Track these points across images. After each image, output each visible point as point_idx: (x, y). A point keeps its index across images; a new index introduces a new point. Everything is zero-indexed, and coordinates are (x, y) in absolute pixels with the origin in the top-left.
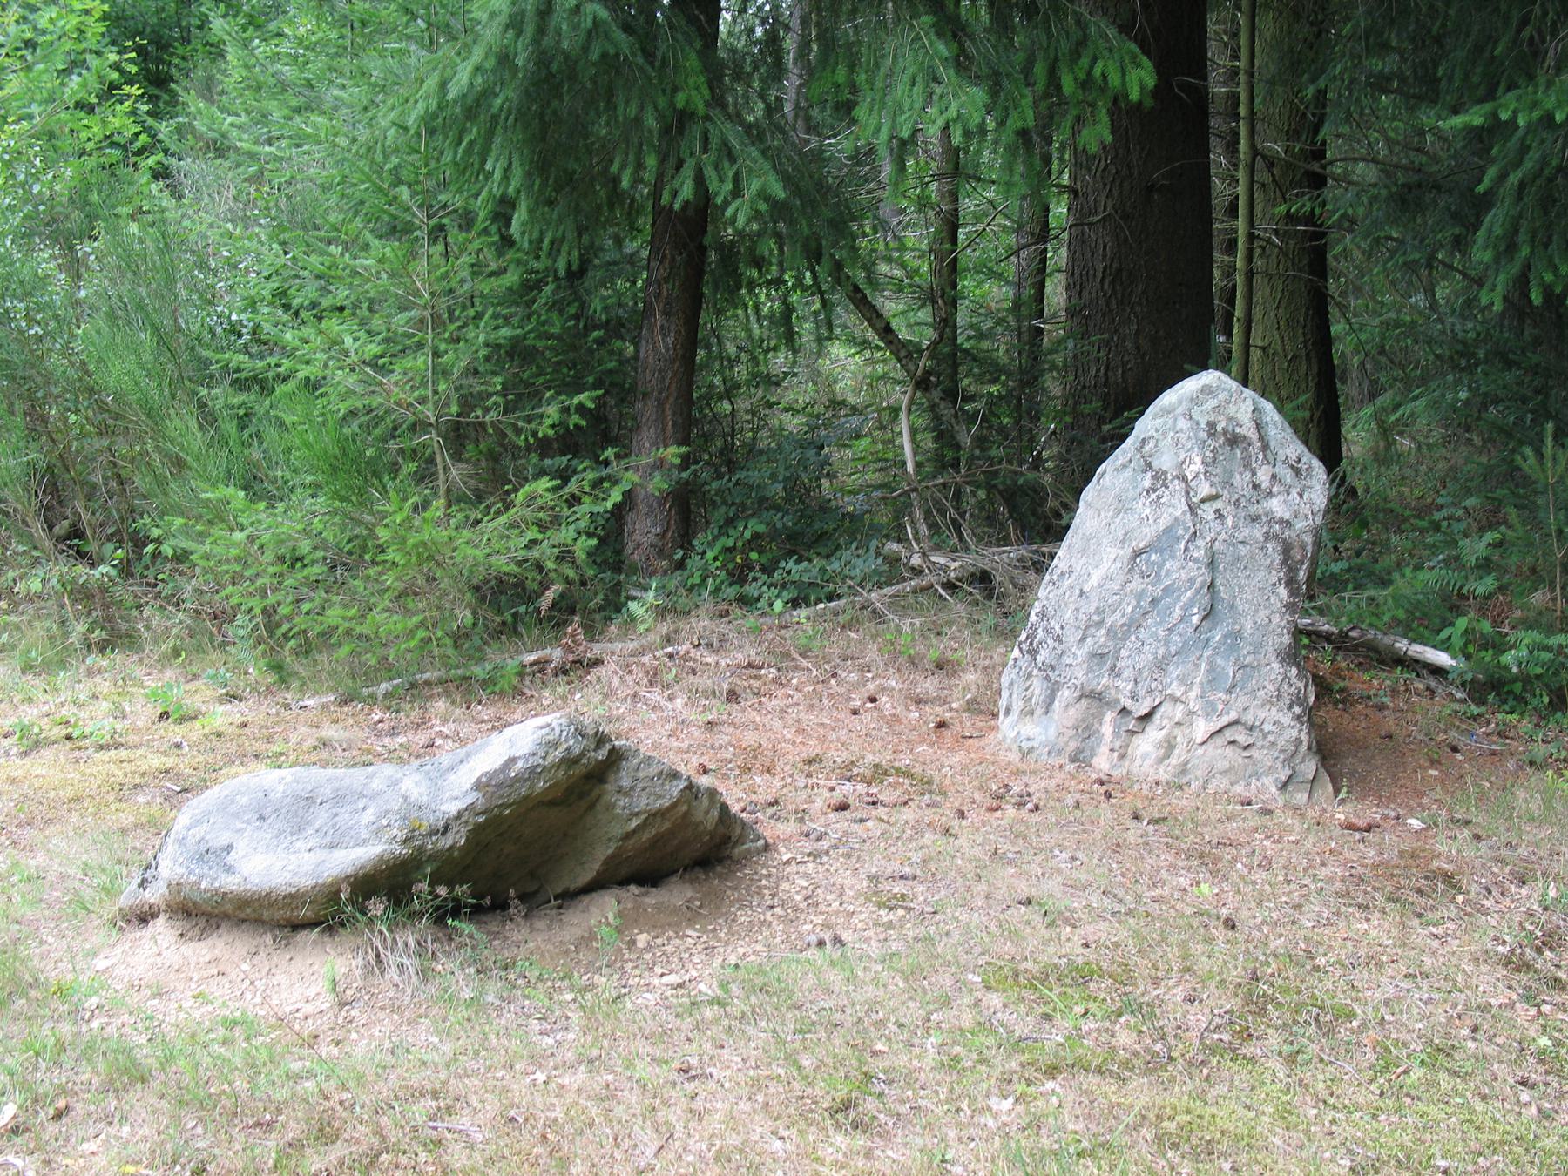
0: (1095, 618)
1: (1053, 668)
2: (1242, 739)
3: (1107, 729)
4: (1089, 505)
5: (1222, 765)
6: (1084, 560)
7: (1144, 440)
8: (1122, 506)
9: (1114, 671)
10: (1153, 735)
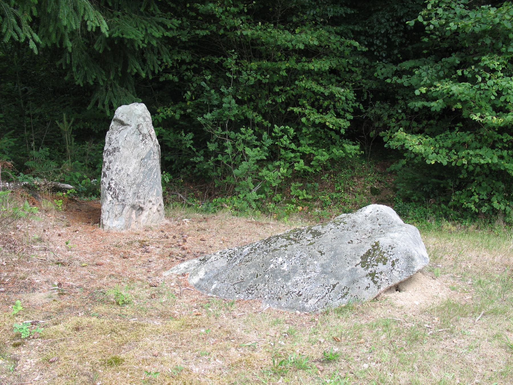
0: (133, 182)
1: (124, 201)
2: (159, 209)
3: (134, 216)
4: (123, 147)
5: (157, 218)
6: (126, 165)
7: (138, 126)
8: (136, 146)
9: (138, 197)
10: (145, 213)
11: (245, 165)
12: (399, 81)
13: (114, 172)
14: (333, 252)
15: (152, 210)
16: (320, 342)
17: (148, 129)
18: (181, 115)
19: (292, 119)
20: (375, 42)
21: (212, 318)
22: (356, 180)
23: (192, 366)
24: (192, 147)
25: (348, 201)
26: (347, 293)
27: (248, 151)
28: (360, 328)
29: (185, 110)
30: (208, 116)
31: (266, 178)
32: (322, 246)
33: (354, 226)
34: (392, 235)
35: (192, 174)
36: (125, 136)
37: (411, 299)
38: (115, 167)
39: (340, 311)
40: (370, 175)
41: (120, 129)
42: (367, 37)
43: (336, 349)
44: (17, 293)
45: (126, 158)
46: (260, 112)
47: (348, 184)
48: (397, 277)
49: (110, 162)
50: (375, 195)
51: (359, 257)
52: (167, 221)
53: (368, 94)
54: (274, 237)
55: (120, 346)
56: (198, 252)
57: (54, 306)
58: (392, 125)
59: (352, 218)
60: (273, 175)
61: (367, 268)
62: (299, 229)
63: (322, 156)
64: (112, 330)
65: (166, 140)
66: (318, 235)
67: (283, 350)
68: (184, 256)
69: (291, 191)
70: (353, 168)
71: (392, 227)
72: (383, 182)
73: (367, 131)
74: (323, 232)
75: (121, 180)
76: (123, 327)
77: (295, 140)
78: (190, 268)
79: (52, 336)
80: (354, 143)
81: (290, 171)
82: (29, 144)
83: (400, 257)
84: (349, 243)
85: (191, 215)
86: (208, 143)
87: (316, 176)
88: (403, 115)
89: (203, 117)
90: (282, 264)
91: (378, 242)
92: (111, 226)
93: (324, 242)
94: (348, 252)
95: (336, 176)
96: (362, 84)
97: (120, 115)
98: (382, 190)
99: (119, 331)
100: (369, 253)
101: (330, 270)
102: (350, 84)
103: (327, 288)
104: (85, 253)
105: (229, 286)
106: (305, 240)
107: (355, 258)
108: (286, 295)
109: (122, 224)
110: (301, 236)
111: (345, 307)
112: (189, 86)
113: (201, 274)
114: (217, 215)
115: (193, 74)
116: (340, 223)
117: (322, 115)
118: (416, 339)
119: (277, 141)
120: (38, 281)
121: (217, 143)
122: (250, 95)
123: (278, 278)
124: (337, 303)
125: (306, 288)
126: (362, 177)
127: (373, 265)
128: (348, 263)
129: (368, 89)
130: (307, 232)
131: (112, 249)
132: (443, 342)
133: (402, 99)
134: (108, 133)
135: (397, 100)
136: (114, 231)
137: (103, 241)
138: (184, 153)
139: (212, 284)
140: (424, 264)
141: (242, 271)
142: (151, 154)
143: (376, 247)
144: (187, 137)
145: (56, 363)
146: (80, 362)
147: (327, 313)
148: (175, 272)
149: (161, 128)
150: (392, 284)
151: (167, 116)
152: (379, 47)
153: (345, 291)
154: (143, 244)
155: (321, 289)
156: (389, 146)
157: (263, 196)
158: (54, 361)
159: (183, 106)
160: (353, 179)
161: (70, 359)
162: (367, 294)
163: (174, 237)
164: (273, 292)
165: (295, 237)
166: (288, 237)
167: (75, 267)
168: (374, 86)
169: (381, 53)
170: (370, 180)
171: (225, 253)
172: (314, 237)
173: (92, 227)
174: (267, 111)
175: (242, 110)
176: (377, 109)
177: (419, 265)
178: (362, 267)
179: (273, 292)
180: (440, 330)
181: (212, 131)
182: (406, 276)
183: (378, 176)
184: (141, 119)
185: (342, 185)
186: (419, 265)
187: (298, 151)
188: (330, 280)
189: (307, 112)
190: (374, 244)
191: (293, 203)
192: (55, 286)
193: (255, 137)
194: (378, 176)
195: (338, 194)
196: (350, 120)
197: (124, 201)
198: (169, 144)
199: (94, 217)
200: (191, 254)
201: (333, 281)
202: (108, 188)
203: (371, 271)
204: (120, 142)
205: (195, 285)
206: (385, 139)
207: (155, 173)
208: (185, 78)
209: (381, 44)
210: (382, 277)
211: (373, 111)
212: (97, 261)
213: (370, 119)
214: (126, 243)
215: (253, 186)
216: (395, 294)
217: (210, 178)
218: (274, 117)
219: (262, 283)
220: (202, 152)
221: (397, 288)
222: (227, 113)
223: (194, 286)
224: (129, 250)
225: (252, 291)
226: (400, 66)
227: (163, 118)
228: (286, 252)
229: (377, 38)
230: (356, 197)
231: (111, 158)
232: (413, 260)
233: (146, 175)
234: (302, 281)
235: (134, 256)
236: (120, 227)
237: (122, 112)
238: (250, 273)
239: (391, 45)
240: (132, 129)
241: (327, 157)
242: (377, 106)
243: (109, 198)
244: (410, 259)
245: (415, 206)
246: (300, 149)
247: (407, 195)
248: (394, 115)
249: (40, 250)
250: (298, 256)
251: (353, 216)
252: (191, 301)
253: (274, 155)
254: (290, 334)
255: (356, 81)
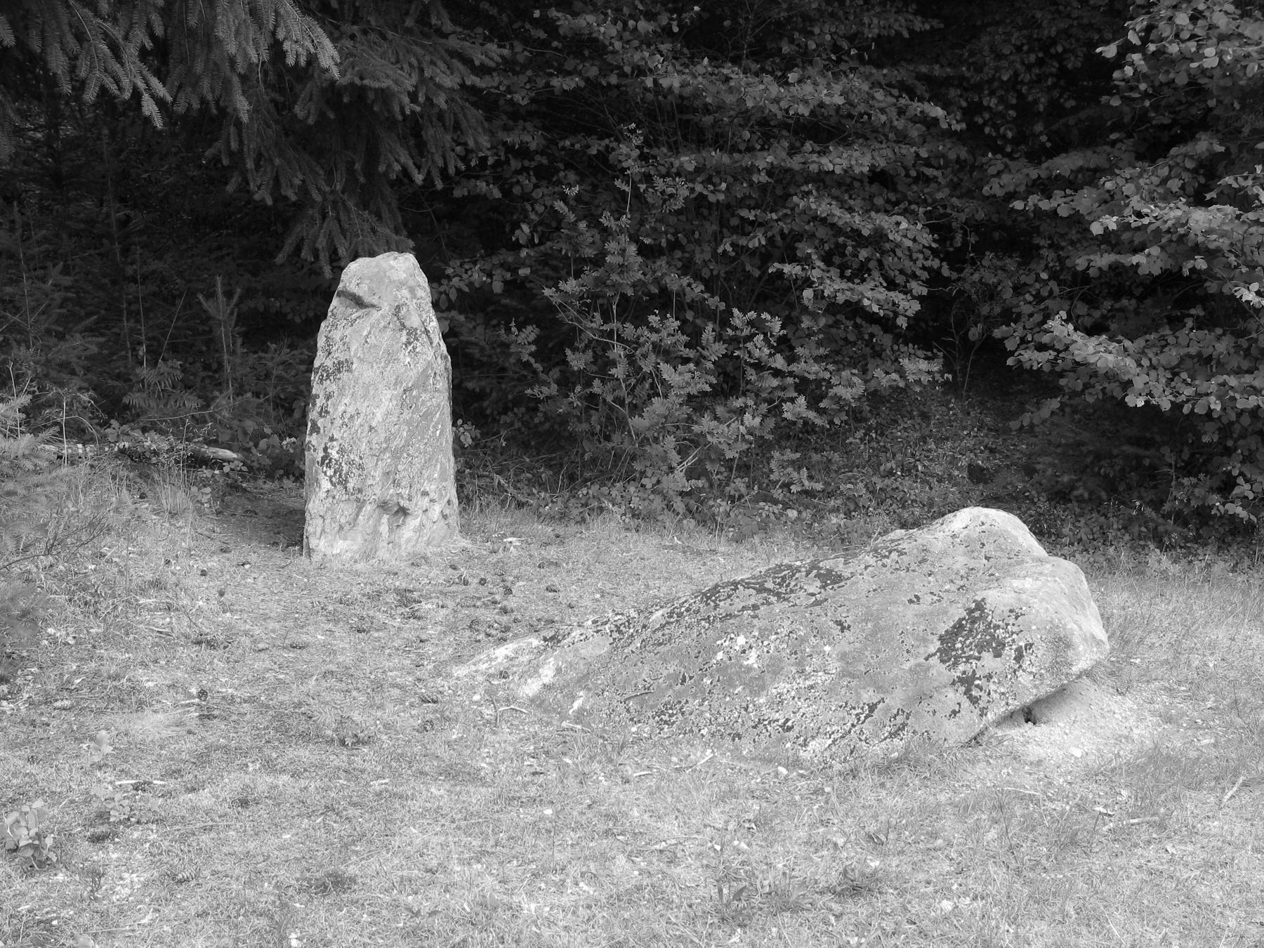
1: (360, 491)
2: (447, 512)
3: (384, 528)
5: (442, 533)
6: (366, 404)
8: (391, 357)
9: (396, 483)
10: (412, 523)
11: (658, 404)
12: (1045, 205)
13: (338, 422)
14: (870, 625)
15: (429, 514)
16: (836, 845)
17: (420, 316)
18: (506, 282)
19: (778, 295)
20: (985, 103)
21: (571, 781)
22: (933, 446)
23: (520, 898)
24: (532, 361)
25: (913, 497)
26: (904, 725)
27: (667, 371)
28: (934, 812)
29: (514, 271)
30: (571, 285)
31: (709, 438)
32: (845, 609)
33: (924, 560)
34: (1016, 583)
35: (525, 425)
36: (365, 333)
37: (1063, 742)
38: (341, 408)
39: (886, 768)
40: (969, 435)
41: (354, 316)
42: (966, 90)
43: (875, 864)
44: (101, 712)
45: (367, 387)
46: (697, 277)
47: (913, 455)
48: (1028, 687)
49: (328, 397)
50: (978, 483)
51: (935, 638)
52: (465, 543)
53: (965, 234)
54: (728, 584)
55: (346, 846)
56: (539, 620)
57: (188, 745)
58: (1026, 309)
59: (920, 541)
60: (728, 431)
61: (955, 664)
62: (789, 567)
63: (848, 388)
64: (326, 807)
65: (469, 343)
66: (834, 582)
67: (743, 863)
68: (507, 629)
69: (771, 471)
70: (925, 416)
71: (1018, 563)
72: (1000, 452)
73: (962, 325)
74: (846, 574)
75: (355, 440)
76: (354, 799)
77: (784, 346)
78: (521, 659)
79: (183, 817)
80: (929, 354)
81: (771, 422)
82: (134, 350)
83: (1036, 638)
84: (911, 601)
85: (524, 529)
86: (568, 352)
87: (835, 436)
88: (1053, 284)
89: (557, 288)
90: (744, 652)
91: (983, 600)
92: (328, 552)
93: (849, 600)
94: (907, 624)
95: (882, 434)
96: (949, 211)
97: (354, 282)
98: (996, 471)
99: (345, 809)
100: (959, 627)
101: (863, 669)
102: (921, 210)
103: (854, 712)
104: (266, 618)
105: (615, 703)
106: (801, 593)
107: (925, 641)
108: (754, 727)
109: (355, 548)
110: (793, 583)
111: (898, 760)
112: (524, 210)
113: (547, 674)
114: (588, 529)
115: (534, 180)
116: (890, 552)
117: (851, 285)
118: (1073, 842)
119: (739, 349)
120: (150, 684)
121: (590, 353)
122: (675, 234)
123: (735, 687)
124: (877, 749)
125: (803, 712)
126: (947, 439)
127: (968, 658)
128: (908, 652)
129: (965, 223)
130: (808, 574)
131: (330, 608)
132: (1139, 851)
133: (1050, 246)
134: (323, 325)
135: (1039, 247)
136: (336, 565)
137: (309, 588)
138: (510, 374)
139: (573, 698)
140: (1096, 657)
141: (647, 668)
142: (428, 377)
143: (977, 614)
144: (523, 335)
145: (193, 883)
146: (250, 883)
147: (854, 773)
148: (483, 667)
149: (454, 313)
150: (1015, 704)
151: (470, 284)
152: (994, 114)
153: (900, 719)
154: (405, 598)
155: (841, 715)
156: (1020, 361)
157: (700, 483)
158: (187, 880)
159: (510, 259)
160: (925, 443)
161: (227, 876)
162: (954, 728)
163: (483, 582)
164: (721, 720)
165: (778, 585)
166: (762, 584)
167: (240, 651)
168: (981, 215)
169: (1002, 130)
170: (966, 446)
171: (606, 623)
172: (824, 587)
173: (280, 554)
174: (715, 273)
175: (654, 272)
176: (989, 271)
177: (1083, 659)
178: (943, 661)
179: (721, 720)
180: (1132, 821)
181: (580, 322)
182: (1049, 685)
183: (986, 435)
184: (405, 292)
185: (899, 457)
186: (1083, 659)
187: (791, 374)
188: (862, 691)
189: (815, 274)
190: (973, 606)
191: (775, 502)
192: (191, 696)
193: (685, 338)
194: (986, 435)
195: (887, 481)
196: (920, 298)
197: (360, 491)
198: (475, 352)
199: (288, 529)
200: (524, 623)
201: (869, 696)
202: (323, 459)
203: (964, 673)
204: (353, 349)
205: (532, 701)
206: (1010, 345)
207: (437, 423)
208: (517, 190)
209: (1001, 108)
210: (992, 687)
211: (976, 277)
212: (294, 637)
213: (969, 296)
214: (364, 595)
215: (678, 458)
216: (1022, 731)
217: (573, 439)
218: (731, 288)
219: (695, 697)
220: (555, 373)
221: (1029, 715)
222: (615, 277)
223: (528, 702)
224: (371, 613)
225: (671, 716)
226: (1047, 168)
227: (459, 290)
228: (755, 621)
229: (992, 93)
230: (931, 488)
231: (332, 387)
232: (1069, 646)
233: (417, 430)
234: (793, 693)
235: (384, 627)
236: (349, 555)
237: (356, 274)
238: (665, 673)
239: (1026, 111)
240: (383, 317)
241: (860, 389)
242: (985, 262)
243: (326, 485)
244: (1061, 643)
245: (1078, 510)
246: (794, 367)
247: (1059, 487)
248: (1031, 285)
249: (157, 609)
250: (784, 632)
251: (923, 536)
252: (521, 740)
253: (730, 381)
254: (762, 822)
255: (935, 201)
